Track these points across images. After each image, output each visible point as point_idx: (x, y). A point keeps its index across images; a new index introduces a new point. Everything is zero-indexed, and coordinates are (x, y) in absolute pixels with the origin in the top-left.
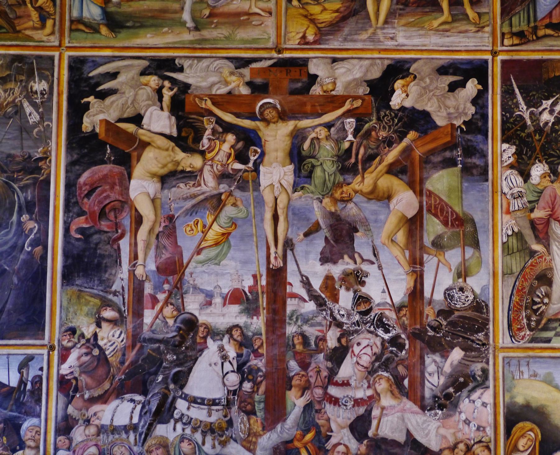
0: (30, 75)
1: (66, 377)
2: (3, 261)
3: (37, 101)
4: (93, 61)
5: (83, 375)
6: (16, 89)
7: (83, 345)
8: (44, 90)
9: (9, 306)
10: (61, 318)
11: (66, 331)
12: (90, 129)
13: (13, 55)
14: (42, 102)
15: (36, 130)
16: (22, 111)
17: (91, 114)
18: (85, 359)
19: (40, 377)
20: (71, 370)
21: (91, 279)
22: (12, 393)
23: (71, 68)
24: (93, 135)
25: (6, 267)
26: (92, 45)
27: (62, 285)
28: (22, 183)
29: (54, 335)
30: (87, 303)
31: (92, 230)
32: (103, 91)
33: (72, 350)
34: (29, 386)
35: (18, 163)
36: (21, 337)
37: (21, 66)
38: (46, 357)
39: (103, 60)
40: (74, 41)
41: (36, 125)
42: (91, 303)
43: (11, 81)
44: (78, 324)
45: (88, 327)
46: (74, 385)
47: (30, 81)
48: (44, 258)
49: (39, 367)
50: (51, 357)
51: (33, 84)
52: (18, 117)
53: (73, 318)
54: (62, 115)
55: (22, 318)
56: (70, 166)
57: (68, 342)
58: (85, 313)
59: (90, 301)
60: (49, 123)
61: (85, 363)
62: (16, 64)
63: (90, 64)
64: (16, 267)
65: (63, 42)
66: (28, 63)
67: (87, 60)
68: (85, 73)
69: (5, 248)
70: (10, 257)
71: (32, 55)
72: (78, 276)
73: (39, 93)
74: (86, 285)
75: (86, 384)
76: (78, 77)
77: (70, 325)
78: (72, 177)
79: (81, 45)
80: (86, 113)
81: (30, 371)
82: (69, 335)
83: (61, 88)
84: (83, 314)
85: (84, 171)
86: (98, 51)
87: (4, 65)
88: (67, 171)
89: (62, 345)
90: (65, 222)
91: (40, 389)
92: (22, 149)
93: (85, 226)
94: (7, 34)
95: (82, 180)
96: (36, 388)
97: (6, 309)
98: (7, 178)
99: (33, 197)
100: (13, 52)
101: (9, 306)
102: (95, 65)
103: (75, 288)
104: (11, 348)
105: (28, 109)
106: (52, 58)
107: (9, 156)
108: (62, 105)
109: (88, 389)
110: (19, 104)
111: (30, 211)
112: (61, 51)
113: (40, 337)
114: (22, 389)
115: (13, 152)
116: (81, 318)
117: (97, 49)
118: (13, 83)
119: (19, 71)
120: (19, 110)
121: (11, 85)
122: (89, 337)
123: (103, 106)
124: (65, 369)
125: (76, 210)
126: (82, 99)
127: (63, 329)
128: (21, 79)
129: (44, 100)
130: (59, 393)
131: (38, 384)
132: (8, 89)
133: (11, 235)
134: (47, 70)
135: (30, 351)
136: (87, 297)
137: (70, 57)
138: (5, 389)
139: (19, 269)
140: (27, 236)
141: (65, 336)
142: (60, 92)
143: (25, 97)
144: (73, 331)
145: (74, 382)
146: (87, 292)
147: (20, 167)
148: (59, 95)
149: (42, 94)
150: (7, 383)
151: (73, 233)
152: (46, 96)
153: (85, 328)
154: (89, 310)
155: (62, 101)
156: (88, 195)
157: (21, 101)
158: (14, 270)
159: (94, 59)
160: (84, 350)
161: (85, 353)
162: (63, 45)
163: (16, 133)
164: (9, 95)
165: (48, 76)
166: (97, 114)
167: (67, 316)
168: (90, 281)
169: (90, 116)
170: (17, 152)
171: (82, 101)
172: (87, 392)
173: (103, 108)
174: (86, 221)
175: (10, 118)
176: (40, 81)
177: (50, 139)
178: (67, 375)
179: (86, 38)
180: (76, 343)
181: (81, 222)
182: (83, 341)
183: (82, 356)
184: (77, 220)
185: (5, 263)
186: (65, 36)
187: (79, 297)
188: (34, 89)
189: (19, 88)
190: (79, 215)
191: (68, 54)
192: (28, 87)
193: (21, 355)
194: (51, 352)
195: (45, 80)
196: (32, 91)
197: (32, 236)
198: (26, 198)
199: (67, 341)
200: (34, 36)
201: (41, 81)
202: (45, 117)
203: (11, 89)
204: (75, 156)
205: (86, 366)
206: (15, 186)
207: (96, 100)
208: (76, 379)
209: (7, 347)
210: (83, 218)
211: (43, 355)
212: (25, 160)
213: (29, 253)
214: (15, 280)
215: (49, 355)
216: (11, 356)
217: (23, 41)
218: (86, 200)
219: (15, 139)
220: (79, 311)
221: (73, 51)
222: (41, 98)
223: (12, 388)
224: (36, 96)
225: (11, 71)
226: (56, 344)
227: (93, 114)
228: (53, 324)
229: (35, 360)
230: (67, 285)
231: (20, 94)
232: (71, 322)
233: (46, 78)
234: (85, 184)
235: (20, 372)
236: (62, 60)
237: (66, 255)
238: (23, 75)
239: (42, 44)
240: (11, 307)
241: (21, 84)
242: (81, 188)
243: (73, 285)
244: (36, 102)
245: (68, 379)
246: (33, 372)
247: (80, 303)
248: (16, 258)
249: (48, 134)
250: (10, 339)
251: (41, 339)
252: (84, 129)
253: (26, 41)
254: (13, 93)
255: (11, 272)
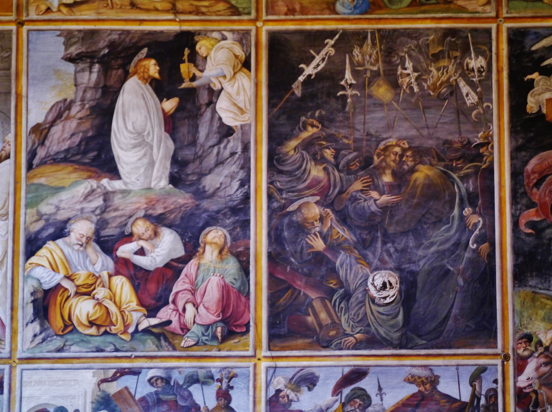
0: (466, 51)
1: (524, 391)
2: (446, 260)
3: (474, 79)
4: (535, 33)
5: (543, 388)
6: (450, 67)
7: (541, 353)
8: (482, 67)
9: (455, 311)
10: (514, 323)
11: (521, 338)
12: (535, 110)
13: (446, 29)
14: (480, 81)
15: (475, 112)
16: (458, 91)
17: (536, 93)
18: (544, 369)
19: (495, 391)
20: (530, 382)
21: (546, 278)
22: (465, 408)
23: (510, 42)
24: (540, 115)
25: (450, 267)
26: (533, 15)
27: (514, 287)
28: (462, 173)
29: (508, 343)
30: (543, 307)
31: (544, 224)
32: (549, 67)
33: (529, 360)
34: (483, 401)
35: (457, 150)
36: (471, 346)
37: (454, 41)
38: (500, 368)
39: (547, 32)
40: (512, 11)
41: (474, 107)
42: (548, 307)
43: (444, 58)
44: (534, 330)
45: (546, 333)
46: (533, 399)
47: (466, 58)
48: (491, 256)
49: (493, 379)
50: (506, 367)
51: (469, 61)
52: (453, 98)
53: (528, 324)
54: (503, 95)
55: (471, 324)
56: (515, 152)
57: (524, 350)
58: (542, 317)
59: (546, 304)
60: (489, 104)
61: (545, 374)
62: (448, 39)
63: (532, 37)
64: (461, 267)
65: (500, 12)
66: (462, 37)
67: (528, 32)
68: (527, 46)
69: (447, 246)
70: (453, 256)
71: (466, 28)
72: (532, 276)
73: (476, 70)
74: (540, 286)
75: (548, 398)
76: (519, 51)
77: (525, 331)
78: (519, 164)
79: (521, 15)
80: (531, 92)
81: (483, 384)
82: (525, 342)
83: (500, 64)
84: (539, 319)
85: (531, 157)
86: (540, 21)
87: (436, 40)
88: (512, 158)
89: (518, 354)
90: (513, 216)
91: (496, 404)
92: (460, 134)
93: (536, 219)
94: (438, 5)
95: (529, 167)
96: (491, 402)
97: (452, 314)
98: (445, 166)
99: (475, 188)
100: (444, 25)
101: (455, 311)
102: (537, 37)
103: (528, 290)
104: (461, 357)
105: (465, 89)
106: (488, 31)
107: (446, 142)
108: (503, 83)
109: (550, 404)
110: (454, 83)
111: (473, 203)
112: (499, 22)
113: (493, 345)
114: (475, 404)
115: (450, 138)
116: (538, 323)
117: (539, 20)
118: (447, 60)
119: (453, 47)
120: (454, 90)
121: (444, 63)
122: (547, 344)
123: (549, 84)
124: (522, 381)
125: (524, 201)
126: (525, 77)
127: (518, 336)
128: (455, 55)
129: (482, 78)
130: (517, 409)
131: (493, 399)
132: (441, 67)
133: (453, 232)
134: (484, 44)
135: (482, 361)
136: (543, 300)
137: (509, 29)
138: (456, 405)
139: (464, 269)
140: (472, 232)
141: (521, 343)
142: (500, 69)
143: (460, 76)
144: (528, 338)
145: (534, 396)
146: (542, 294)
147: (459, 154)
148: (499, 72)
149: (479, 71)
150: (458, 398)
151: (522, 227)
152: (484, 74)
153: (542, 335)
154: (545, 313)
155: (503, 79)
156: (538, 185)
157: (456, 80)
158: (459, 270)
159: (536, 30)
160: (542, 360)
161: (544, 363)
162: (500, 15)
163: (454, 116)
164: (443, 74)
165: (485, 51)
166: (542, 93)
167: (521, 321)
168: (545, 281)
169: (535, 95)
170: (455, 138)
171: (526, 79)
172: (549, 407)
173: (550, 86)
174: (537, 214)
175: (445, 99)
176: (477, 57)
177: (491, 122)
178: (525, 388)
179: (526, 7)
180: (533, 352)
181: (530, 215)
182: (541, 350)
183: (541, 366)
184: (526, 212)
185: (448, 263)
186: (502, 6)
187: (533, 300)
188: (471, 66)
189: (453, 65)
190: (528, 207)
191: (506, 26)
192: (463, 64)
193: (472, 365)
194: (505, 363)
195: (482, 55)
196: (468, 69)
197: (477, 232)
198: (467, 190)
199: (522, 349)
200: (468, 7)
201: (478, 57)
202: (484, 97)
203: (444, 67)
204: (521, 141)
205: (546, 378)
206: (455, 176)
207: (540, 77)
208: (535, 392)
209: (455, 357)
210: (533, 210)
211: (497, 365)
212: (464, 146)
213: (474, 251)
214: (461, 281)
215: (503, 365)
216: (460, 367)
217: (455, 13)
218: (535, 190)
219: (451, 123)
220: (534, 316)
221: (511, 22)
222: (479, 77)
223: (464, 403)
224: (472, 74)
225: (443, 47)
226: (510, 352)
227: (538, 92)
228: (506, 331)
229: (488, 371)
230: (519, 286)
231: (455, 72)
232: (526, 328)
233: (483, 54)
234: (533, 172)
235: (471, 385)
236: (500, 33)
237: (516, 252)
238: (457, 50)
239: (477, 15)
240: (457, 311)
241: (455, 61)
242: (528, 177)
243: (526, 286)
244: (473, 81)
245: (526, 393)
246: (486, 385)
247: (535, 307)
248: (459, 257)
249: (488, 117)
250: (458, 348)
251: (493, 348)
252: (528, 110)
253: (459, 13)
254: (447, 72)
255: (456, 272)
